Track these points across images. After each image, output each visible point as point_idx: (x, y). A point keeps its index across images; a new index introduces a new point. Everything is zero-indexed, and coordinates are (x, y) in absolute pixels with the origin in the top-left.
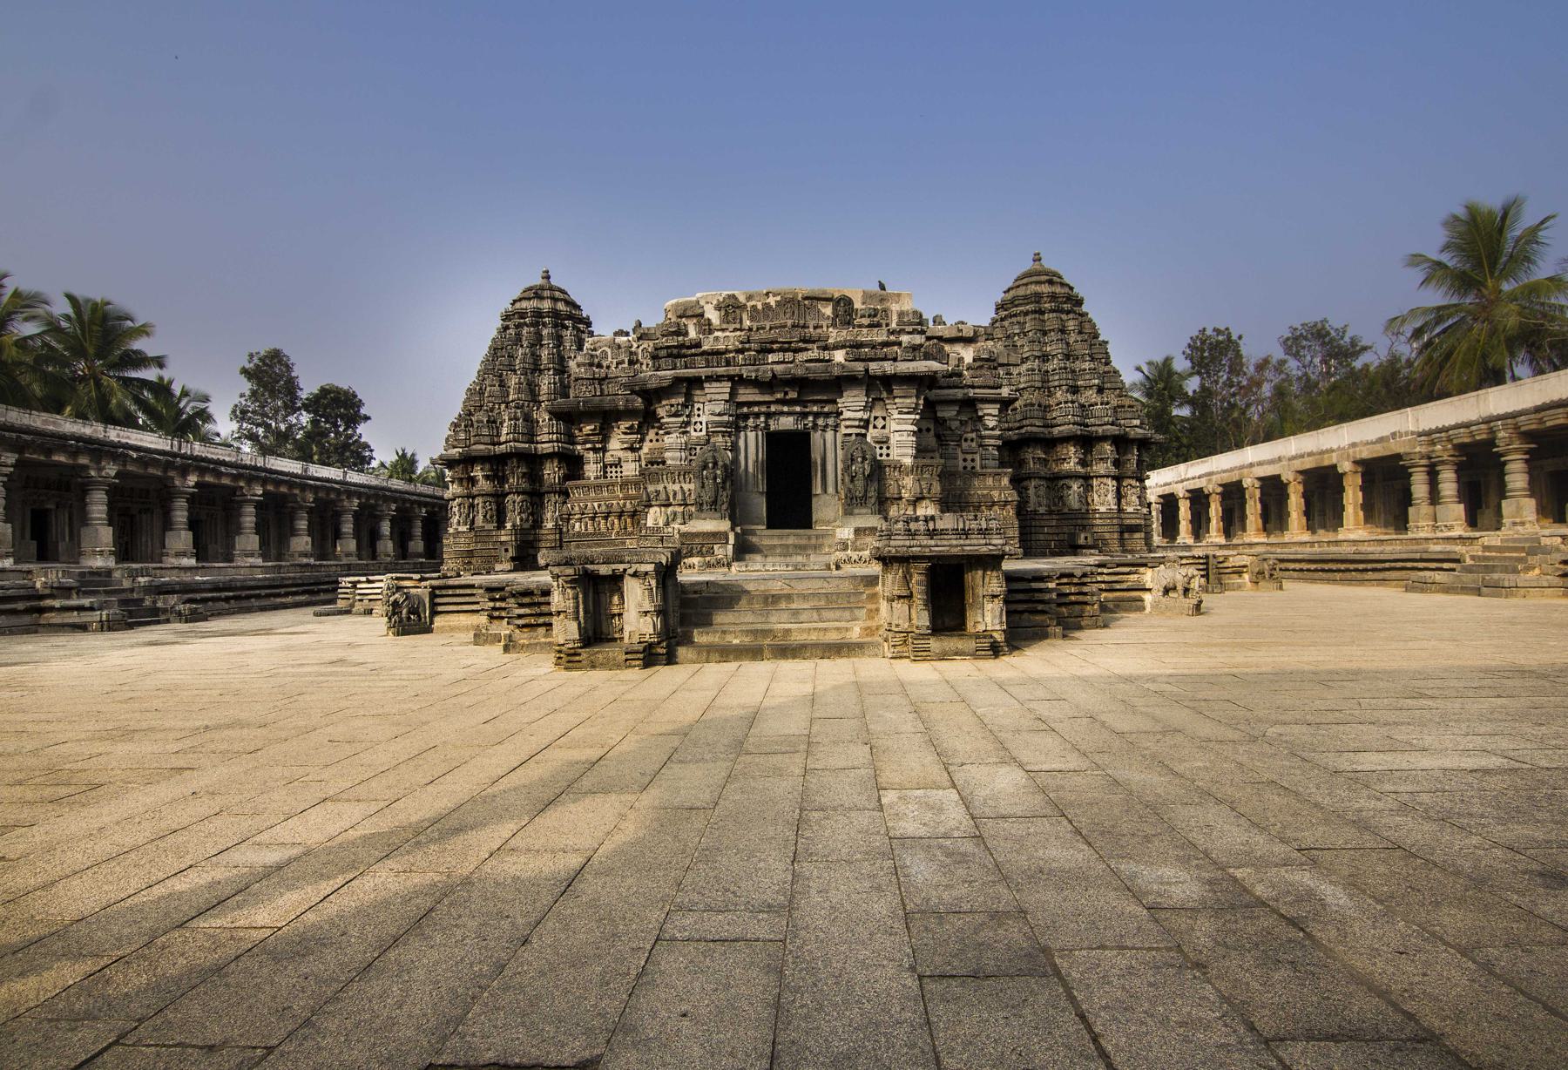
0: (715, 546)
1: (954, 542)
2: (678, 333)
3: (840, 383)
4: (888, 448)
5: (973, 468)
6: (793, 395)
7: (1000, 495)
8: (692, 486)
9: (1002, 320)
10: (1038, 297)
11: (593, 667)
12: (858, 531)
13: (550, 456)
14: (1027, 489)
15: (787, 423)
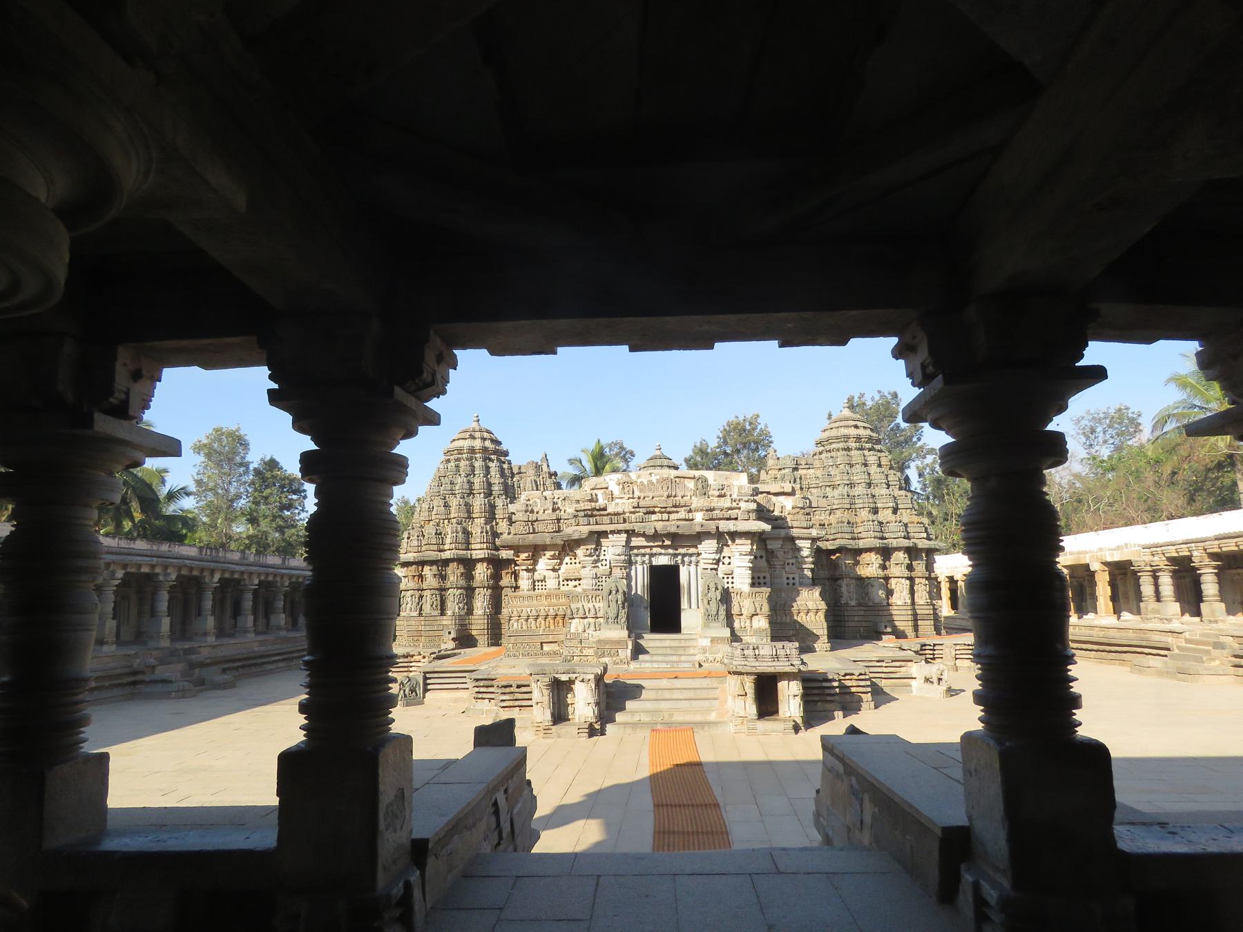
0: (619, 650)
1: (770, 664)
2: (591, 501)
3: (700, 537)
4: (732, 578)
5: (794, 584)
6: (667, 543)
7: (813, 605)
8: (601, 605)
9: (821, 453)
10: (847, 438)
11: (559, 737)
12: (713, 640)
13: (481, 560)
14: (841, 587)
15: (663, 560)
